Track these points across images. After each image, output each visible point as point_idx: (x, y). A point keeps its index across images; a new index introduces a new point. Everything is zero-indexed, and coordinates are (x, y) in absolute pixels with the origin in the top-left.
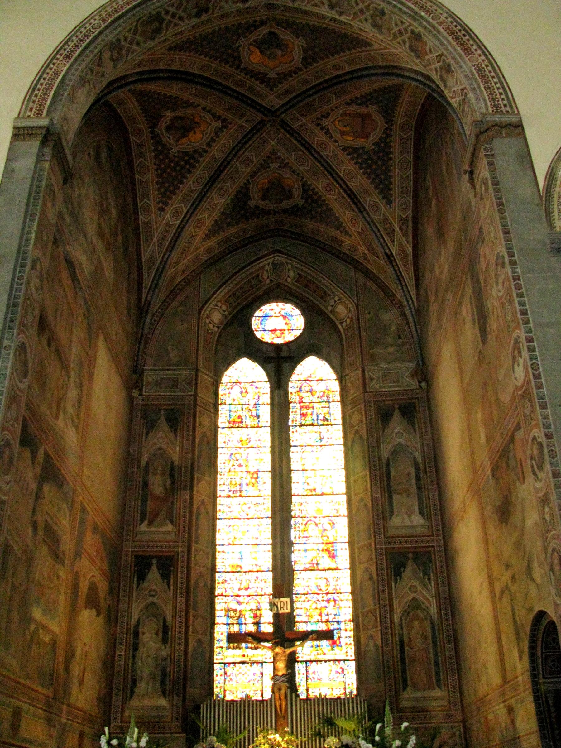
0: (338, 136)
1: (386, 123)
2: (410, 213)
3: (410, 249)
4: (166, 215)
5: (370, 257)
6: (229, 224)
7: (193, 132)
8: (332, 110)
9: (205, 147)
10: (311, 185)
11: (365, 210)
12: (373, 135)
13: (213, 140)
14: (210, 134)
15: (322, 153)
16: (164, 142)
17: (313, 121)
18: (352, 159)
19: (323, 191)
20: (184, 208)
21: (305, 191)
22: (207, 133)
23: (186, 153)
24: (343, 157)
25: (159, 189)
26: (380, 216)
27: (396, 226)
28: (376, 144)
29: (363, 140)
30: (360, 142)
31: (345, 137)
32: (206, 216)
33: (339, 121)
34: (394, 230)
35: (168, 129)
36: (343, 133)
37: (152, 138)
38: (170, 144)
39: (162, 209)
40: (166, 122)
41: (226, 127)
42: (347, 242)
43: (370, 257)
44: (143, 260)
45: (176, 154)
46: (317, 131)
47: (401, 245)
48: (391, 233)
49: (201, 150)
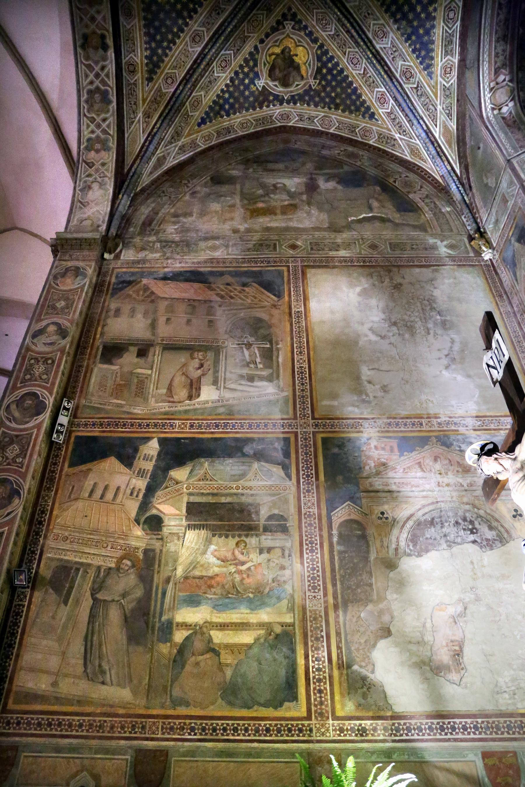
4: (379, 114)
6: (428, 32)
7: (295, 58)
9: (317, 46)
13: (310, 34)
14: (302, 37)
16: (301, 91)
20: (380, 89)
22: (300, 41)
23: (319, 70)
25: (351, 112)
32: (401, 62)
35: (285, 84)
37: (295, 103)
38: (305, 85)
39: (372, 116)
40: (276, 86)
41: (294, 15)
44: (409, 158)
45: (318, 81)
49: (319, 52)
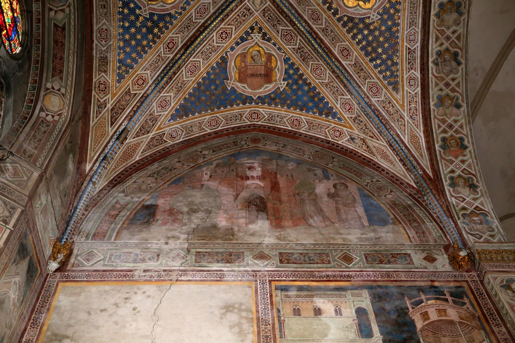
0: (239, 50)
1: (259, 97)
2: (170, 143)
3: (137, 159)
5: (106, 112)
8: (274, 44)
10: (172, 24)
11: (160, 93)
12: (244, 87)
15: (214, 33)
17: (257, 23)
18: (213, 68)
19: (167, 40)
21: (162, 17)
24: (214, 59)
26: (158, 112)
27: (153, 133)
28: (233, 90)
29: (237, 76)
30: (233, 72)
31: (239, 59)
33: (259, 51)
34: (148, 132)
36: (243, 56)
42: (111, 78)
43: (106, 112)
46: (246, 26)
47: (137, 145)
48: (144, 130)
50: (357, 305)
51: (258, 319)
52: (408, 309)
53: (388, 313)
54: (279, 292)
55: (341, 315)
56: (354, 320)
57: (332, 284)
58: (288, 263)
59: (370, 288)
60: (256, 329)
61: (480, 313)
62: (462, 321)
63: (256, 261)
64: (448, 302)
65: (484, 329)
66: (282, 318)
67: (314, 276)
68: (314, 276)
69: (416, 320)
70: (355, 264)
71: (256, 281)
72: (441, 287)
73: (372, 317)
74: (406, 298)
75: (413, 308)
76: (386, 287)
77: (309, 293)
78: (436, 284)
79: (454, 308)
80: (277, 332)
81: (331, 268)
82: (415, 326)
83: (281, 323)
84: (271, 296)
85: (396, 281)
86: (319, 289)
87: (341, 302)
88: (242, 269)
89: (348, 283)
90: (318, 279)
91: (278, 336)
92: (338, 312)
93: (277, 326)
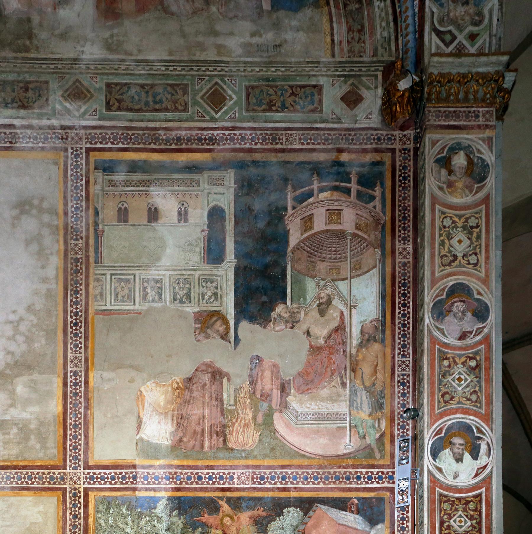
50: (213, 201)
51: (66, 228)
52: (286, 209)
53: (256, 217)
54: (99, 174)
55: (186, 221)
56: (202, 231)
57: (183, 158)
58: (119, 109)
59: (241, 166)
60: (62, 248)
61: (388, 218)
62: (357, 232)
63: (68, 105)
64: (350, 196)
65: (382, 247)
66: (101, 227)
67: (156, 140)
68: (156, 140)
69: (291, 232)
70: (226, 113)
71: (66, 150)
72: (350, 163)
73: (230, 225)
74: (289, 187)
75: (294, 208)
76: (265, 164)
77: (145, 178)
78: (345, 157)
79: (355, 207)
80: (92, 253)
81: (186, 120)
82: (287, 242)
83: (98, 234)
84: (87, 182)
85: (283, 151)
86: (161, 167)
87: (191, 195)
88: (45, 122)
89: (207, 155)
90: (163, 147)
91: (92, 260)
92: (183, 215)
93: (92, 241)
